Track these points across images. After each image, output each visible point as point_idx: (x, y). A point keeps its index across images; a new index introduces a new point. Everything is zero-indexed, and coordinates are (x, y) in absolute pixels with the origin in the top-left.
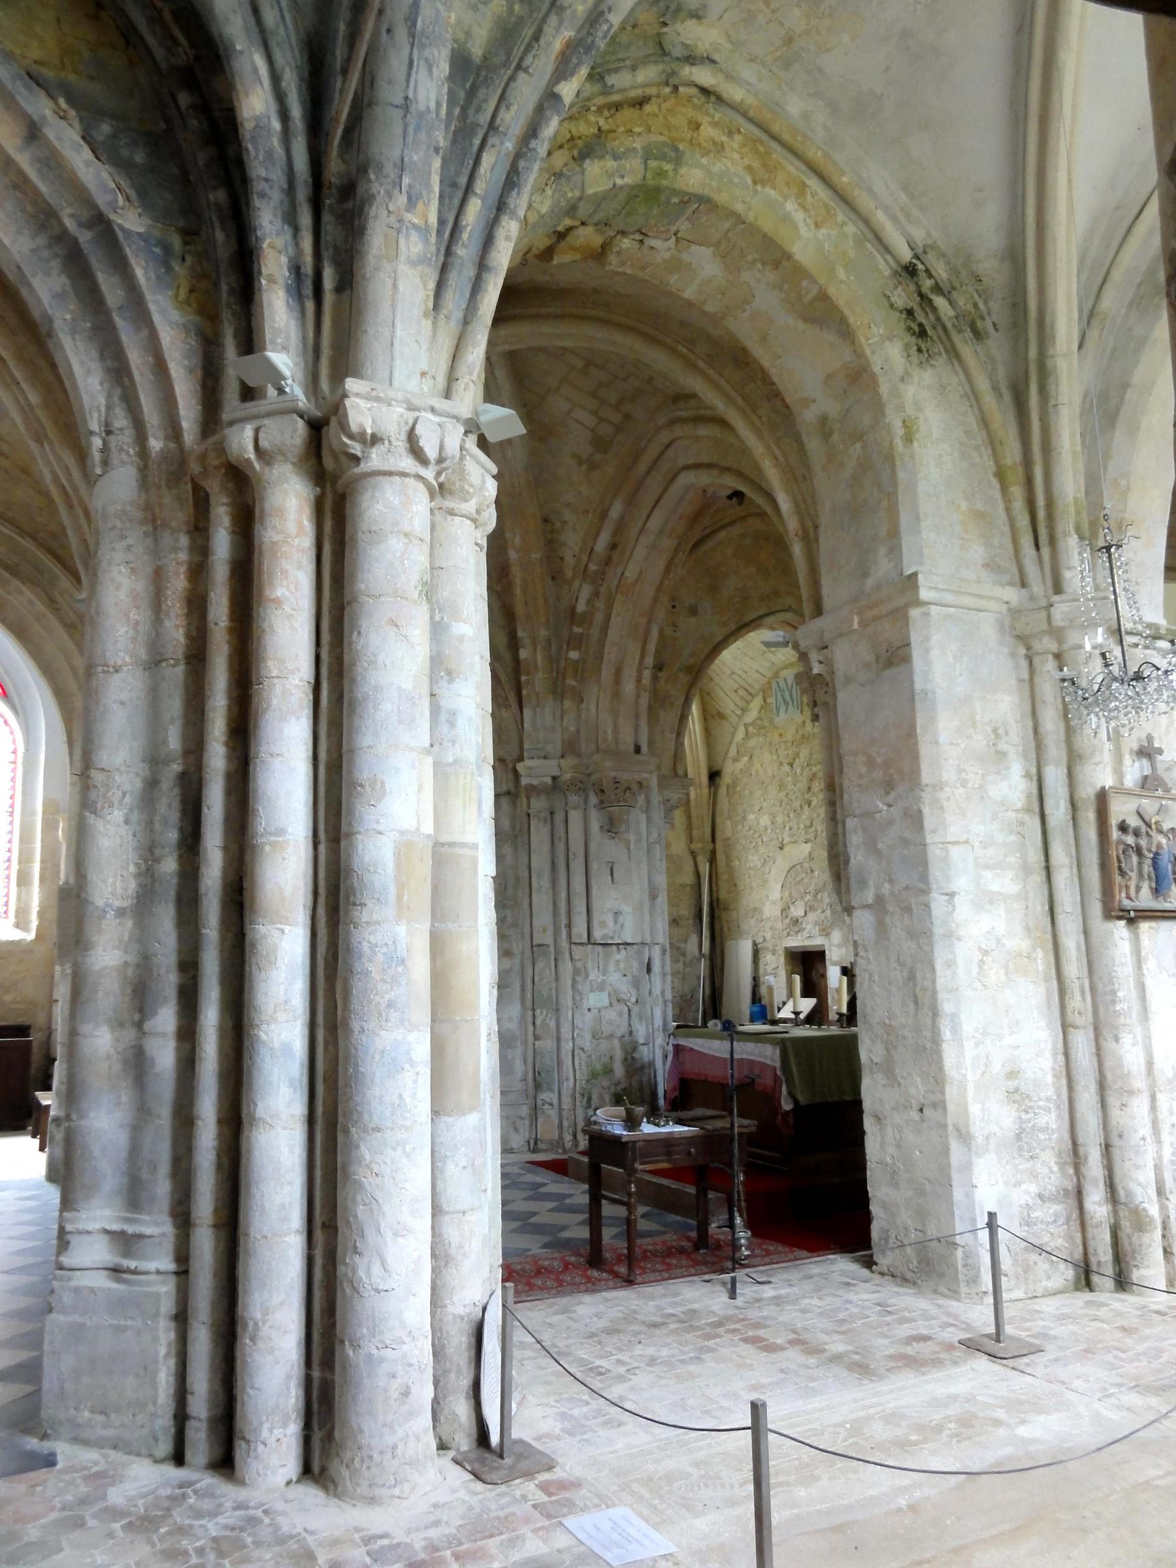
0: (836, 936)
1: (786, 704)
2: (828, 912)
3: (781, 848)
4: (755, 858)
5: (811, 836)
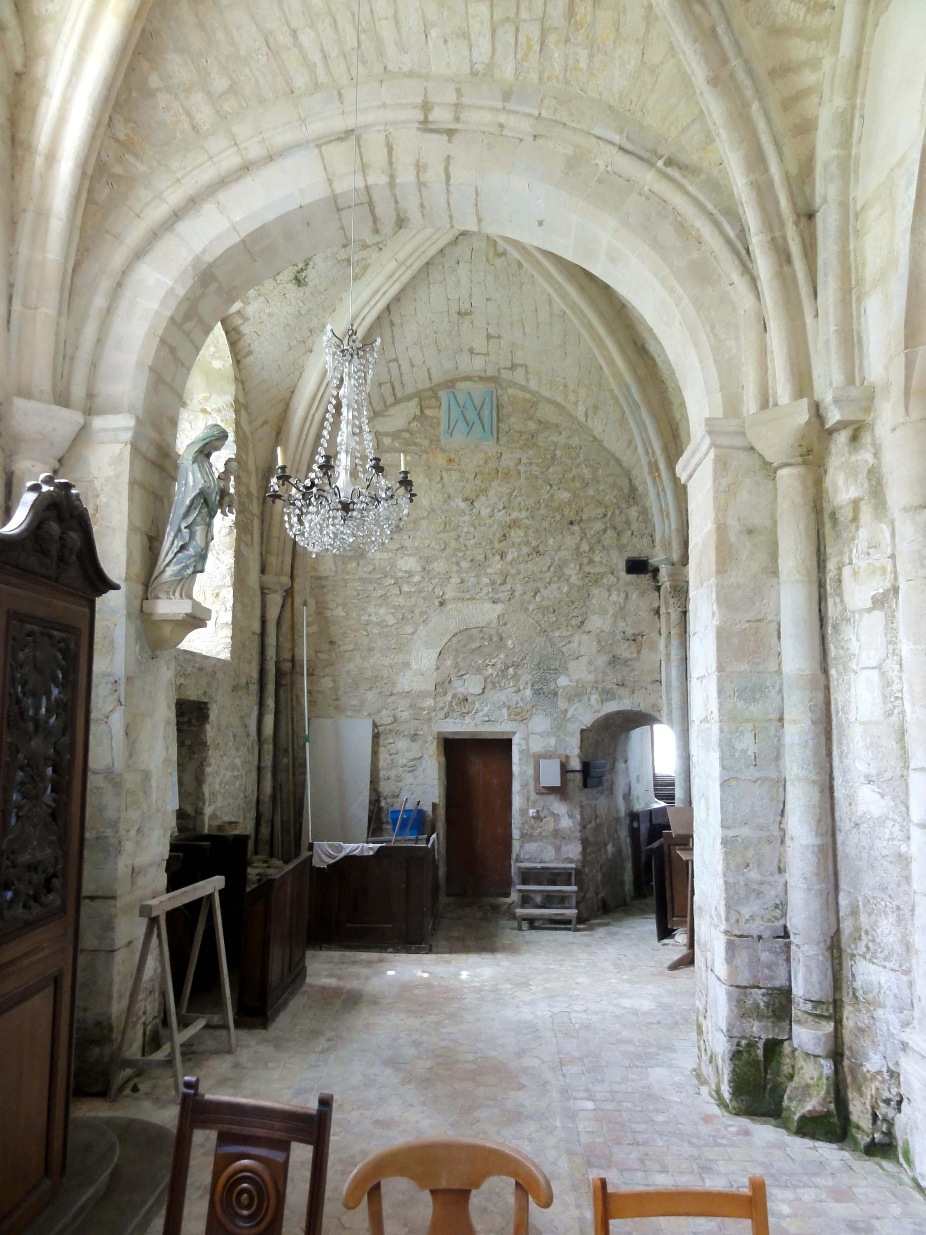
0: (540, 722)
1: (469, 425)
2: (528, 692)
3: (442, 604)
4: (382, 611)
5: (503, 596)
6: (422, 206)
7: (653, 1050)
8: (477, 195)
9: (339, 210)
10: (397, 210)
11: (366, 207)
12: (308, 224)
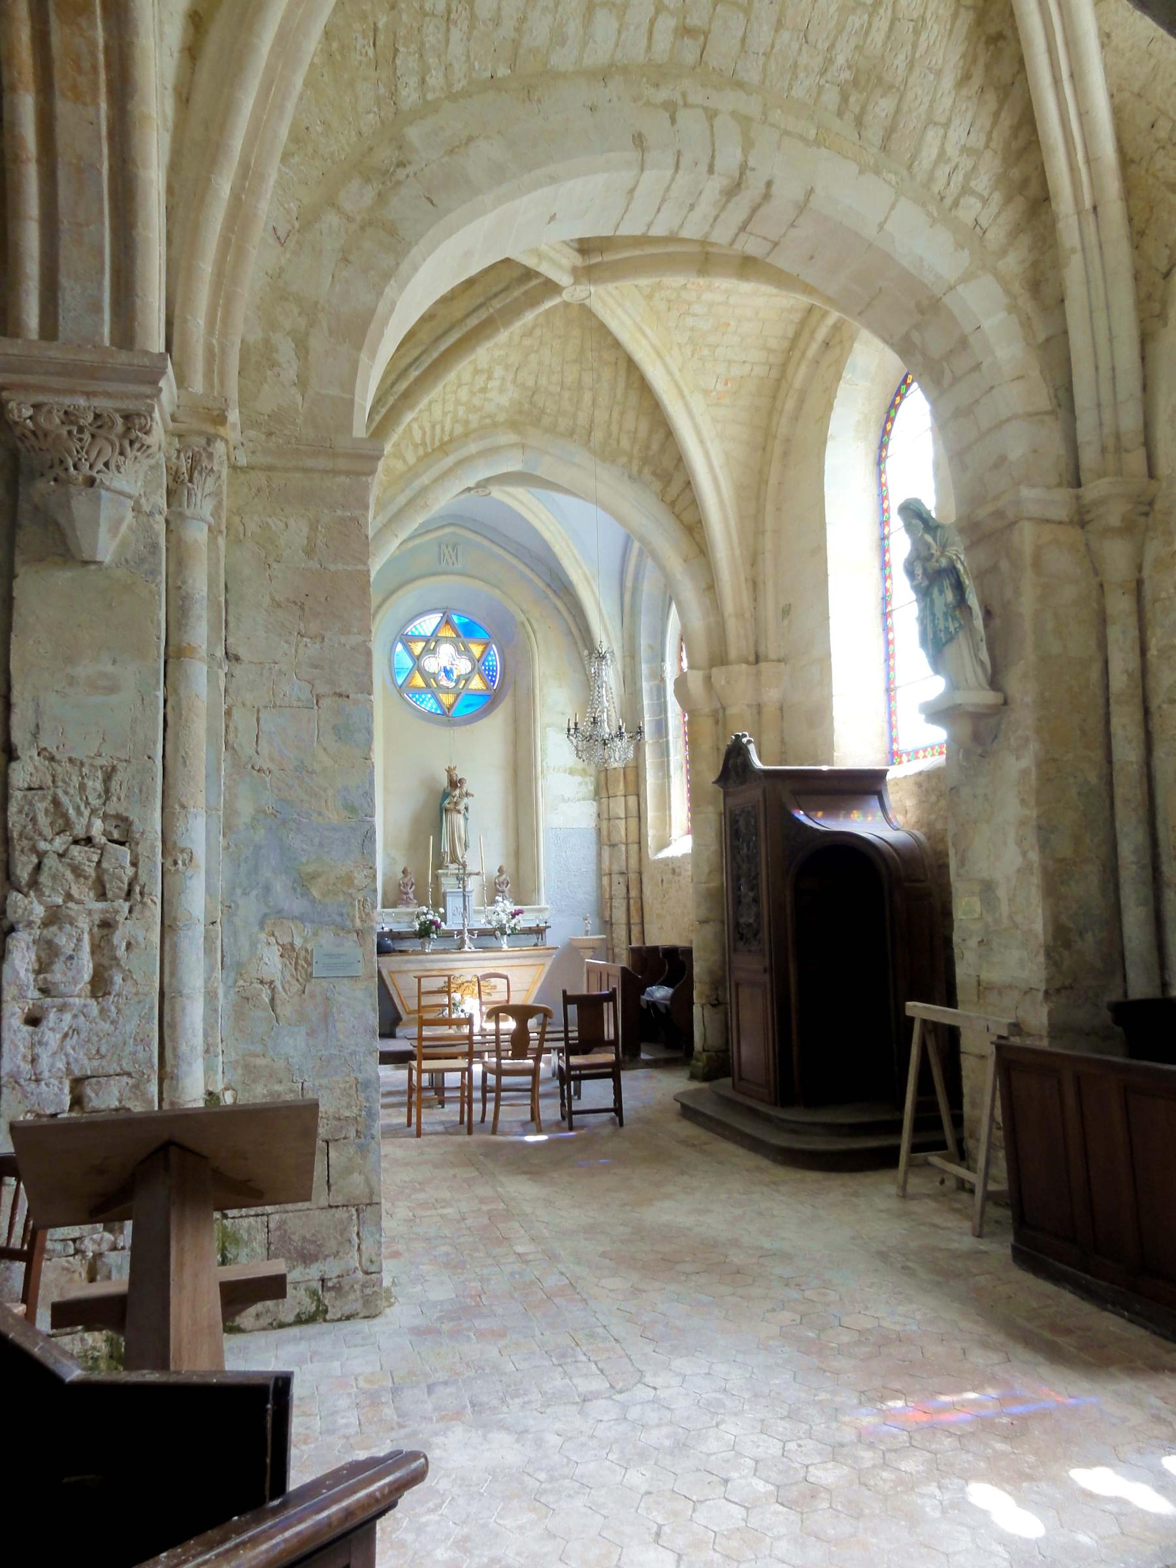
6: (692, 207)
7: (446, 1327)
8: (618, 225)
9: (776, 244)
10: (724, 207)
11: (748, 229)
12: (812, 258)
